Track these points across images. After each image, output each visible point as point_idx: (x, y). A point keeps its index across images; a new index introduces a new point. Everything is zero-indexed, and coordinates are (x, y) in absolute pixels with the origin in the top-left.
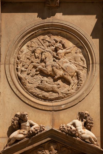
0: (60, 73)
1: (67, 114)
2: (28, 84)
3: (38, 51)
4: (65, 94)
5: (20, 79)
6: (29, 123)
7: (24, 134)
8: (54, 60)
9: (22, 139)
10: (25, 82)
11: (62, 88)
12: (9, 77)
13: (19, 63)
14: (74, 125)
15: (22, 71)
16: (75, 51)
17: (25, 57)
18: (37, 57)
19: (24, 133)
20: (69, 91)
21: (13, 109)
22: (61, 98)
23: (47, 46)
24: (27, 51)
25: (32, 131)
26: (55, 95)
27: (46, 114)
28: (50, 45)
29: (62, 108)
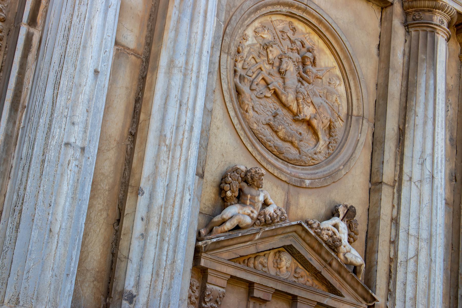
0: (308, 112)
1: (311, 201)
2: (251, 112)
3: (274, 52)
4: (310, 157)
5: (238, 92)
6: (264, 196)
7: (252, 218)
8: (299, 81)
9: (247, 227)
10: (248, 105)
11: (305, 144)
12: (225, 82)
13: (238, 61)
14: (336, 226)
15: (242, 78)
16: (328, 80)
17: (249, 53)
18: (271, 62)
19: (252, 215)
20: (315, 154)
21: (223, 155)
22: (303, 164)
23: (288, 49)
24: (253, 41)
25: (270, 216)
26: (292, 153)
27: (277, 187)
28: (295, 48)
29: (306, 184)
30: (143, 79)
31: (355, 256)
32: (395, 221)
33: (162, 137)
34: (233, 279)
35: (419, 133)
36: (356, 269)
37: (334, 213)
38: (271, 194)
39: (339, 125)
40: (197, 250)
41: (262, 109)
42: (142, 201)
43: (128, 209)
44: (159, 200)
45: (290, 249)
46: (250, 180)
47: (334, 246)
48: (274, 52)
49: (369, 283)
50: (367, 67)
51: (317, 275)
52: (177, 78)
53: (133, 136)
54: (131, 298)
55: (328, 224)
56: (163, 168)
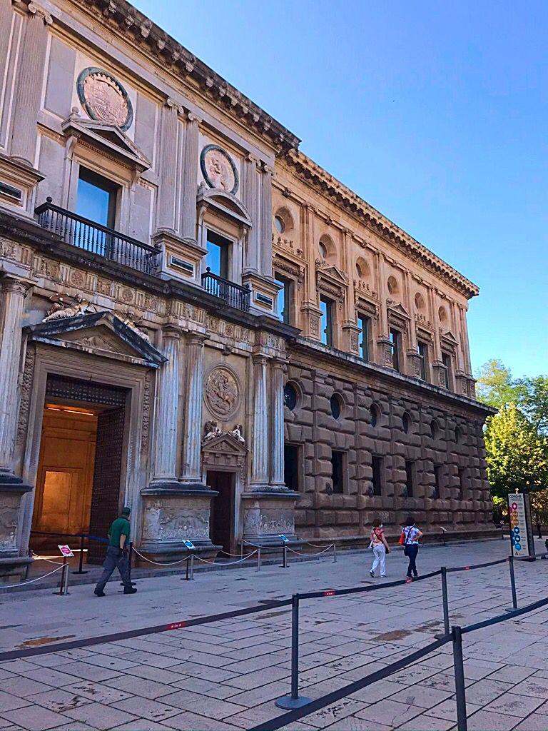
3: (216, 382)
5: (208, 397)
30: (185, 403)
31: (243, 440)
32: (253, 426)
33: (192, 421)
34: (211, 453)
35: (259, 398)
36: (243, 443)
37: (235, 428)
38: (219, 426)
39: (235, 398)
40: (202, 448)
41: (215, 399)
42: (189, 439)
43: (185, 441)
44: (193, 438)
45: (225, 441)
46: (215, 425)
47: (237, 438)
48: (216, 382)
49: (247, 446)
50: (243, 379)
51: (232, 446)
52: (195, 402)
53: (184, 420)
54: (189, 465)
55: (234, 432)
56: (193, 429)
